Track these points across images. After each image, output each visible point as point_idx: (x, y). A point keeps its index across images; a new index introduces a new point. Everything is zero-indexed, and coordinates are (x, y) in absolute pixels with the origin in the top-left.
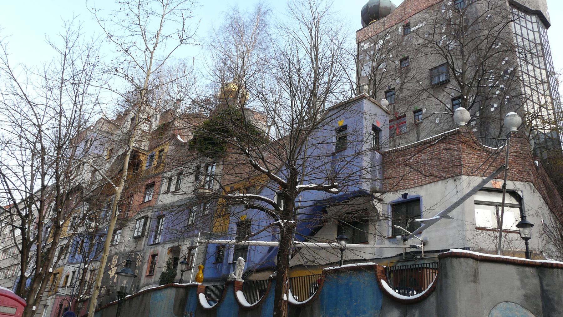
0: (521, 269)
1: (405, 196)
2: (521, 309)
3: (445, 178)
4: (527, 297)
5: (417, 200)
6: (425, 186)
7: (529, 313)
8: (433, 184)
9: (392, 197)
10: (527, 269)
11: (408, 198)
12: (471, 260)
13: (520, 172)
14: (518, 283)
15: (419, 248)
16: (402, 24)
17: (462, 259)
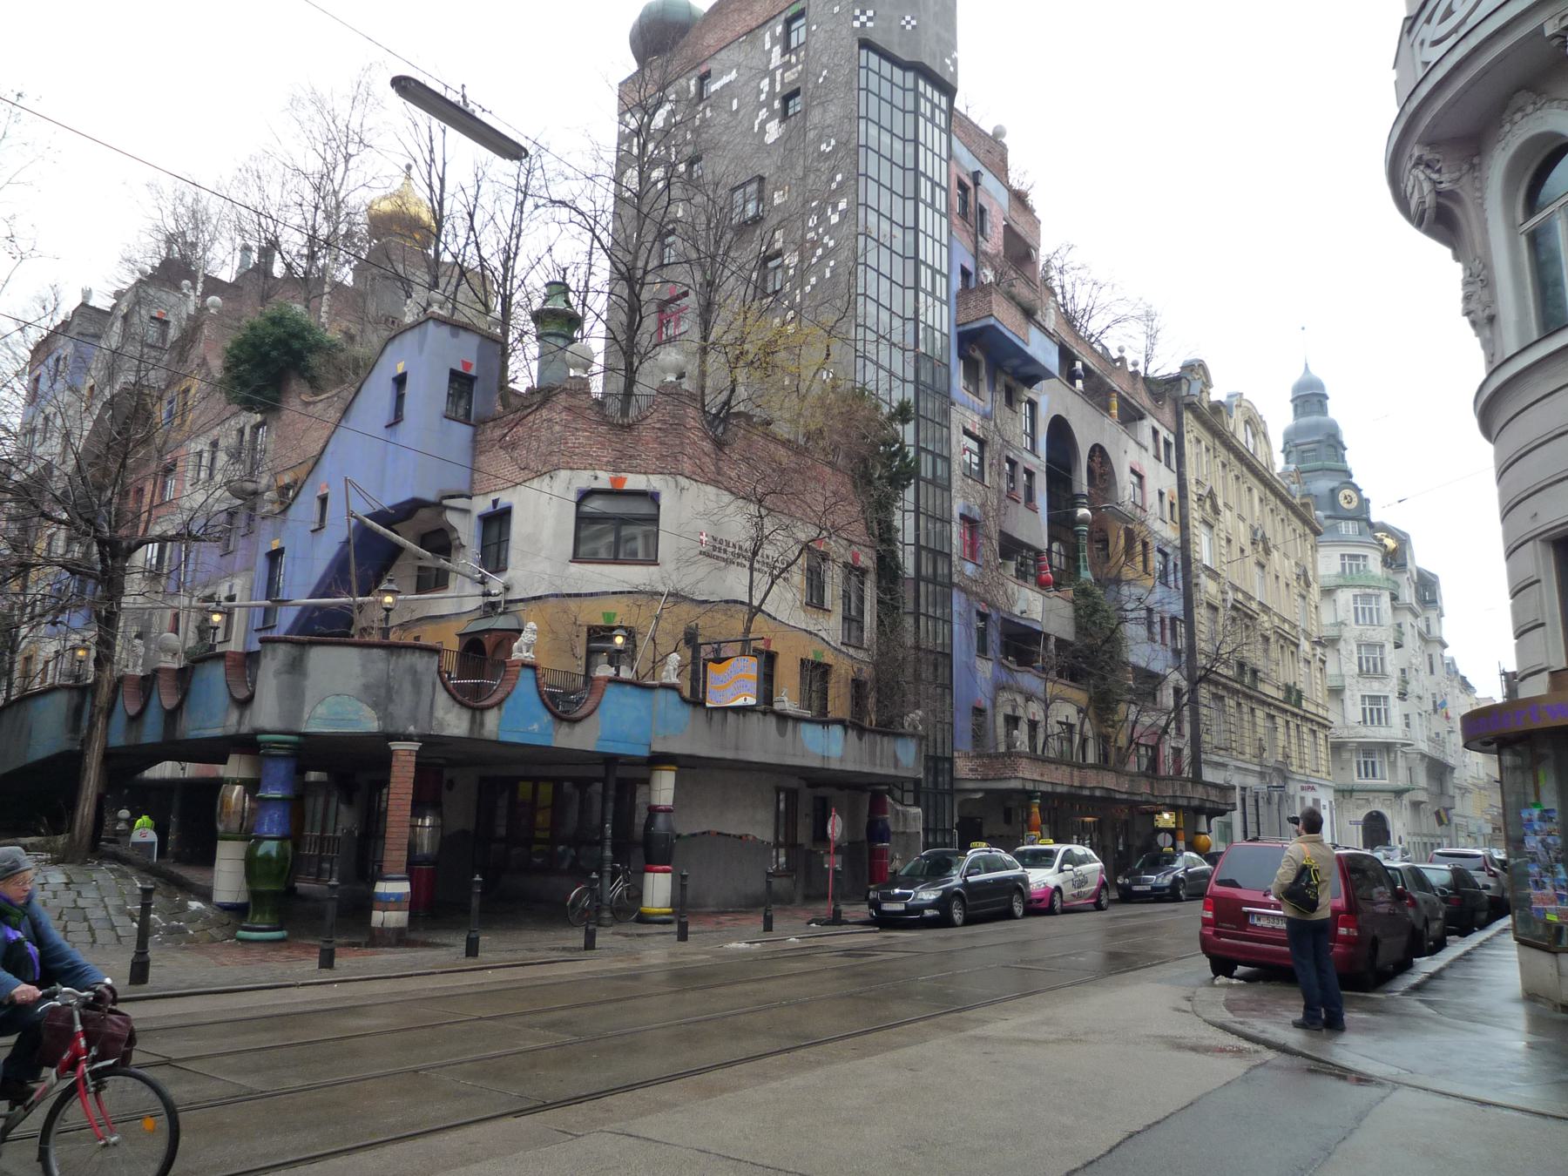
0: (365, 651)
1: (495, 502)
4: (366, 687)
7: (365, 707)
9: (482, 505)
13: (662, 457)
14: (358, 670)
16: (697, 73)
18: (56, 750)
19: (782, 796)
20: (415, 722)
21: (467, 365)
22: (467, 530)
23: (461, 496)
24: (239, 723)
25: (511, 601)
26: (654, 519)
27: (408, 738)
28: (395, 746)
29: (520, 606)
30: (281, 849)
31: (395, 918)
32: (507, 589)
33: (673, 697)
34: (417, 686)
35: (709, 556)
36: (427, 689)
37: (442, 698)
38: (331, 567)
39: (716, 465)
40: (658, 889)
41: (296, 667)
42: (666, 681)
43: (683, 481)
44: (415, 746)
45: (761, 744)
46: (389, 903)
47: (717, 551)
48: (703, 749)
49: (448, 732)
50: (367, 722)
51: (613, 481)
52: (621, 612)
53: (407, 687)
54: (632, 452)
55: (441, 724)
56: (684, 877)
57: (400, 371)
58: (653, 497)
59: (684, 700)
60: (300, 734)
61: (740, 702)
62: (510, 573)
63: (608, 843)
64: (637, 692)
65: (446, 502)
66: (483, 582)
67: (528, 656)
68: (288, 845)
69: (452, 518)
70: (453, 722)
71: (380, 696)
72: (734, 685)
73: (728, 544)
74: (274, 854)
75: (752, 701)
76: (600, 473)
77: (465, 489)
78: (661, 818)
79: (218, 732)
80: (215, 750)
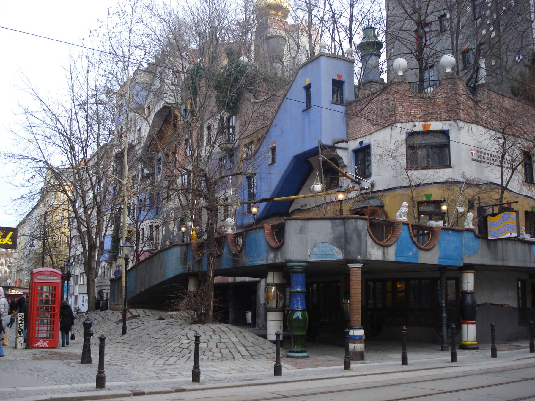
0: (333, 221)
1: (361, 143)
2: (331, 246)
3: (386, 127)
5: (368, 147)
6: (373, 134)
7: (335, 248)
8: (378, 132)
9: (354, 145)
10: (337, 221)
11: (363, 146)
12: (299, 221)
13: (447, 112)
14: (330, 230)
15: (367, 189)
17: (293, 221)
18: (177, 273)
19: (519, 282)
20: (360, 253)
21: (340, 76)
22: (346, 158)
23: (343, 142)
24: (275, 258)
25: (375, 192)
26: (447, 146)
27: (357, 262)
28: (351, 266)
29: (380, 194)
30: (303, 315)
31: (359, 346)
32: (372, 185)
33: (471, 235)
34: (359, 236)
35: (476, 160)
36: (363, 238)
37: (370, 241)
38: (280, 182)
39: (476, 113)
40: (470, 332)
41: (302, 231)
42: (467, 227)
43: (461, 124)
44: (360, 265)
45: (515, 258)
46: (355, 339)
47: (481, 158)
48: (487, 261)
49: (373, 258)
50: (338, 255)
51: (424, 126)
52: (436, 194)
53: (355, 237)
54: (432, 111)
55: (370, 254)
56: (492, 326)
57: (307, 82)
58: (445, 133)
59: (476, 236)
60: (306, 262)
61: (508, 235)
62: (372, 178)
63: (444, 310)
64: (455, 234)
65: (336, 145)
66: (359, 183)
67: (404, 219)
68: (306, 312)
69: (340, 153)
70: (376, 253)
71: (342, 241)
72: (504, 227)
73: (485, 154)
74: (301, 317)
75: (514, 235)
76: (417, 123)
77: (344, 137)
78: (469, 297)
79: (264, 262)
80: (262, 271)
